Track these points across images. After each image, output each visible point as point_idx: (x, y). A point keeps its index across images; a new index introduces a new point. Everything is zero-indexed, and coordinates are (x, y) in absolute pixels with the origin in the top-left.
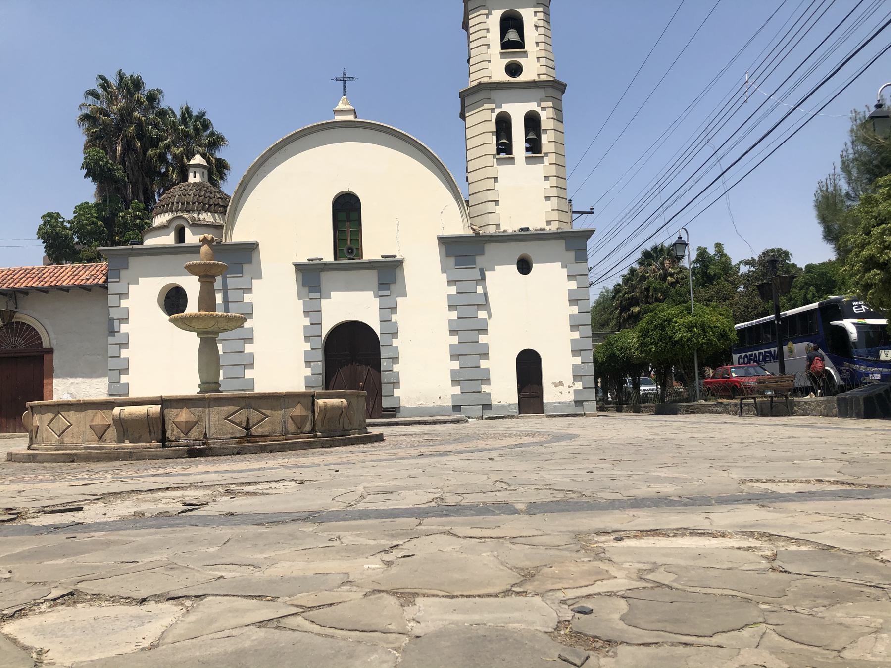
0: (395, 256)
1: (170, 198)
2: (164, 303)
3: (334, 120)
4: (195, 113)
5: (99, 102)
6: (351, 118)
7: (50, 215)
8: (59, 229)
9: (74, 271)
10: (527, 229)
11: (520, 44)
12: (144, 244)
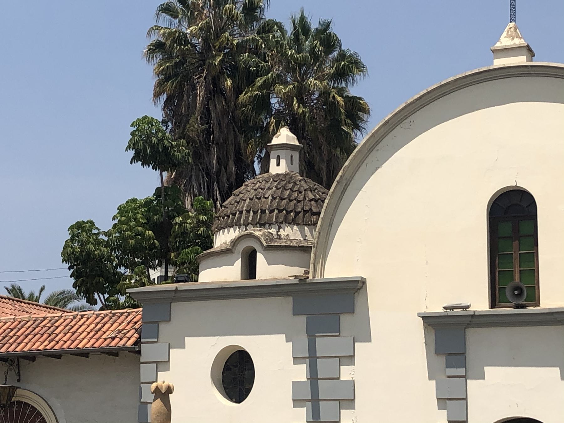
1: (238, 203)
2: (221, 377)
3: (492, 67)
4: (314, 26)
5: (177, 21)
6: (521, 60)
7: (80, 225)
8: (91, 247)
9: (98, 323)
12: (200, 280)
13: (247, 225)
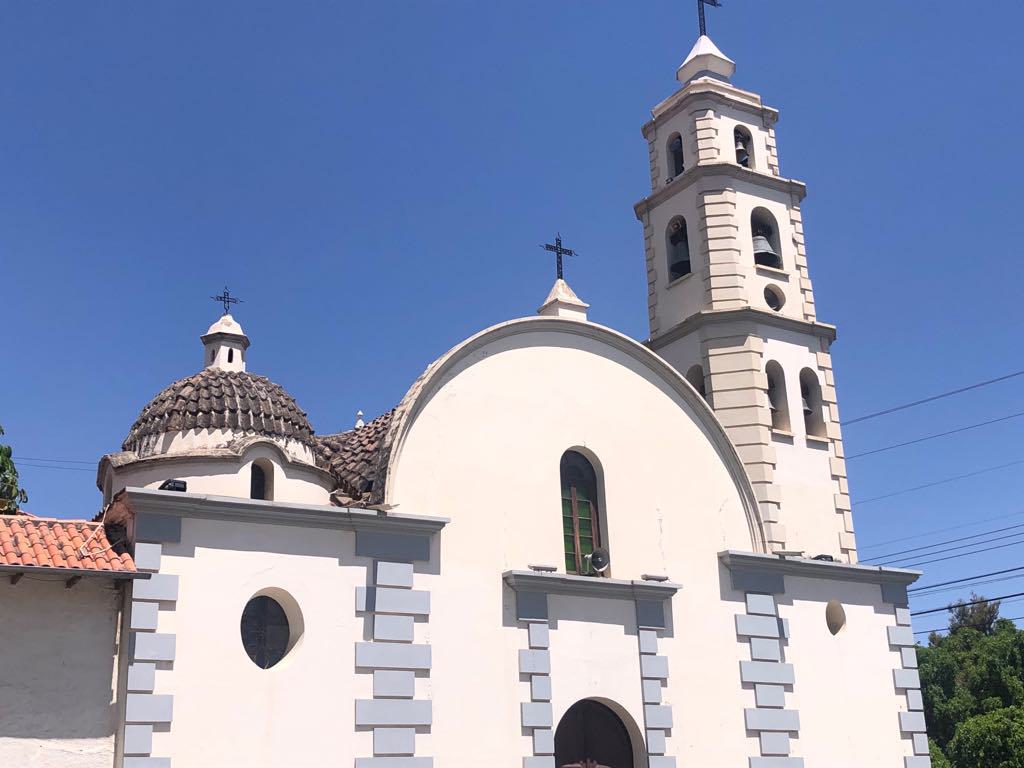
10: (830, 558)
13: (247, 430)
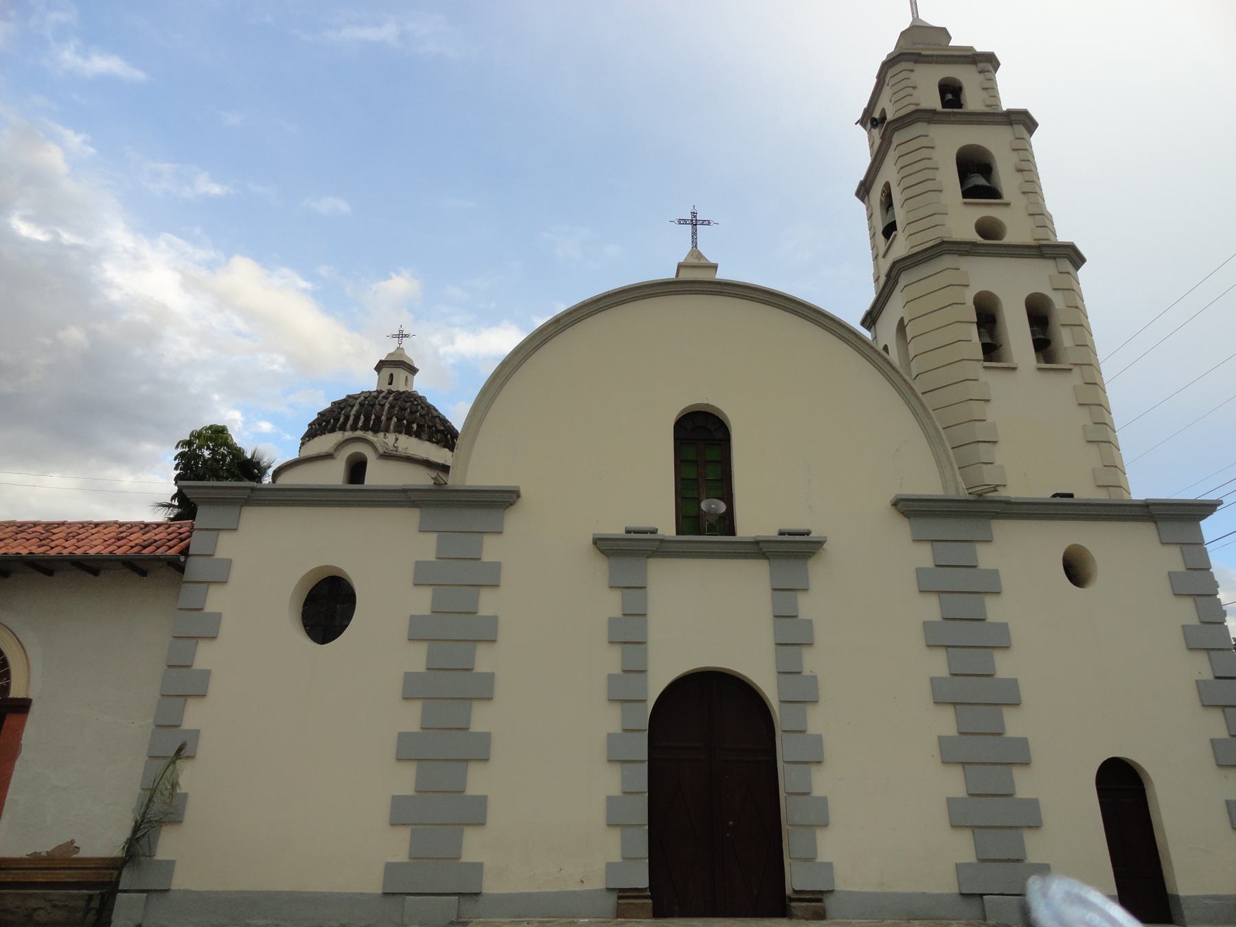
0: (808, 533)
10: (1071, 496)
11: (991, 193)
